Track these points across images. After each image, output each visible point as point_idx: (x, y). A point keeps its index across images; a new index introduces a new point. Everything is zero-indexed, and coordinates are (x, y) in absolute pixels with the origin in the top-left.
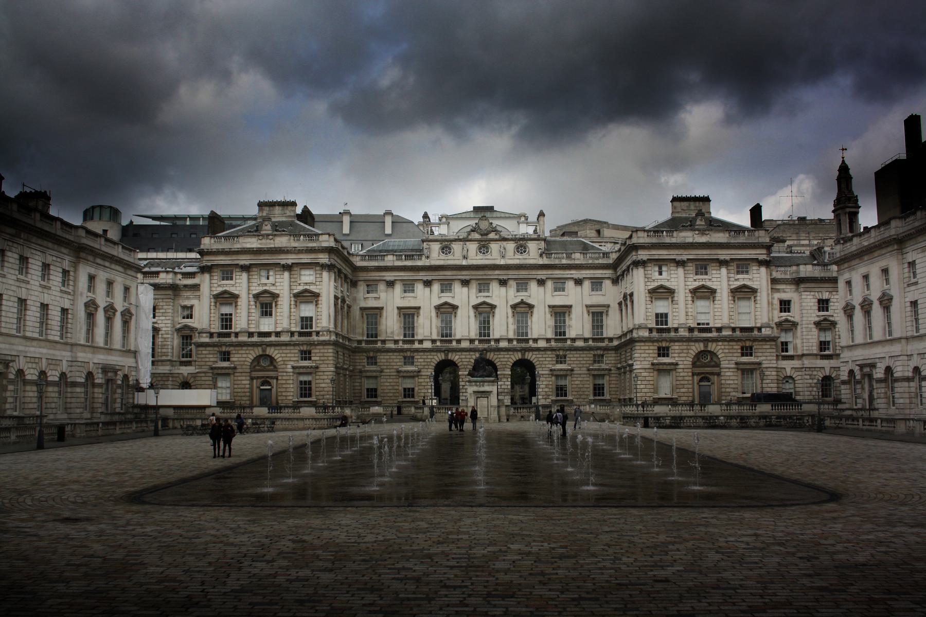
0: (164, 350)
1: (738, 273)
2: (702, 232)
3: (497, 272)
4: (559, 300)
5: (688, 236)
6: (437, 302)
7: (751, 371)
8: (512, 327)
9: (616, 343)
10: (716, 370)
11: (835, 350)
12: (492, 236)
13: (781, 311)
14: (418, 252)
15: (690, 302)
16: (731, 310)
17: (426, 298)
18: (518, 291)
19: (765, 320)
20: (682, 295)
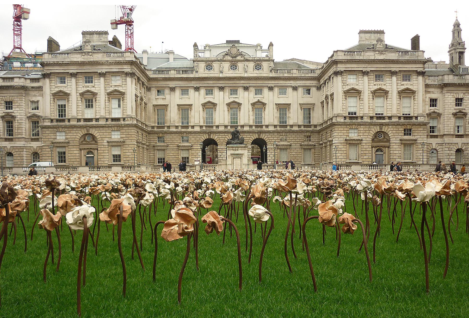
0: (19, 131)
1: (403, 80)
2: (381, 52)
3: (242, 82)
4: (282, 101)
5: (370, 55)
7: (410, 145)
8: (252, 118)
9: (319, 128)
10: (387, 144)
11: (465, 131)
12: (239, 58)
13: (431, 106)
14: (192, 70)
15: (371, 99)
16: (399, 105)
17: (197, 99)
18: (256, 94)
19: (421, 112)
20: (366, 95)
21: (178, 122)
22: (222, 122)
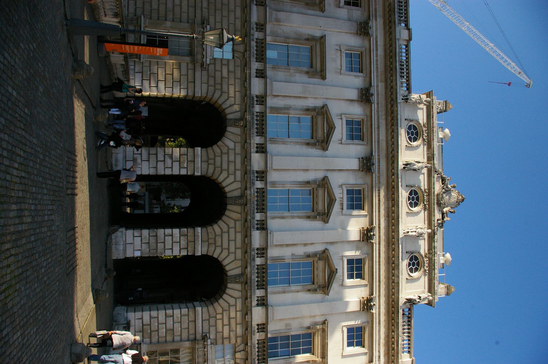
6: (335, 109)
8: (287, 252)
21: (274, 34)
22: (276, 162)
